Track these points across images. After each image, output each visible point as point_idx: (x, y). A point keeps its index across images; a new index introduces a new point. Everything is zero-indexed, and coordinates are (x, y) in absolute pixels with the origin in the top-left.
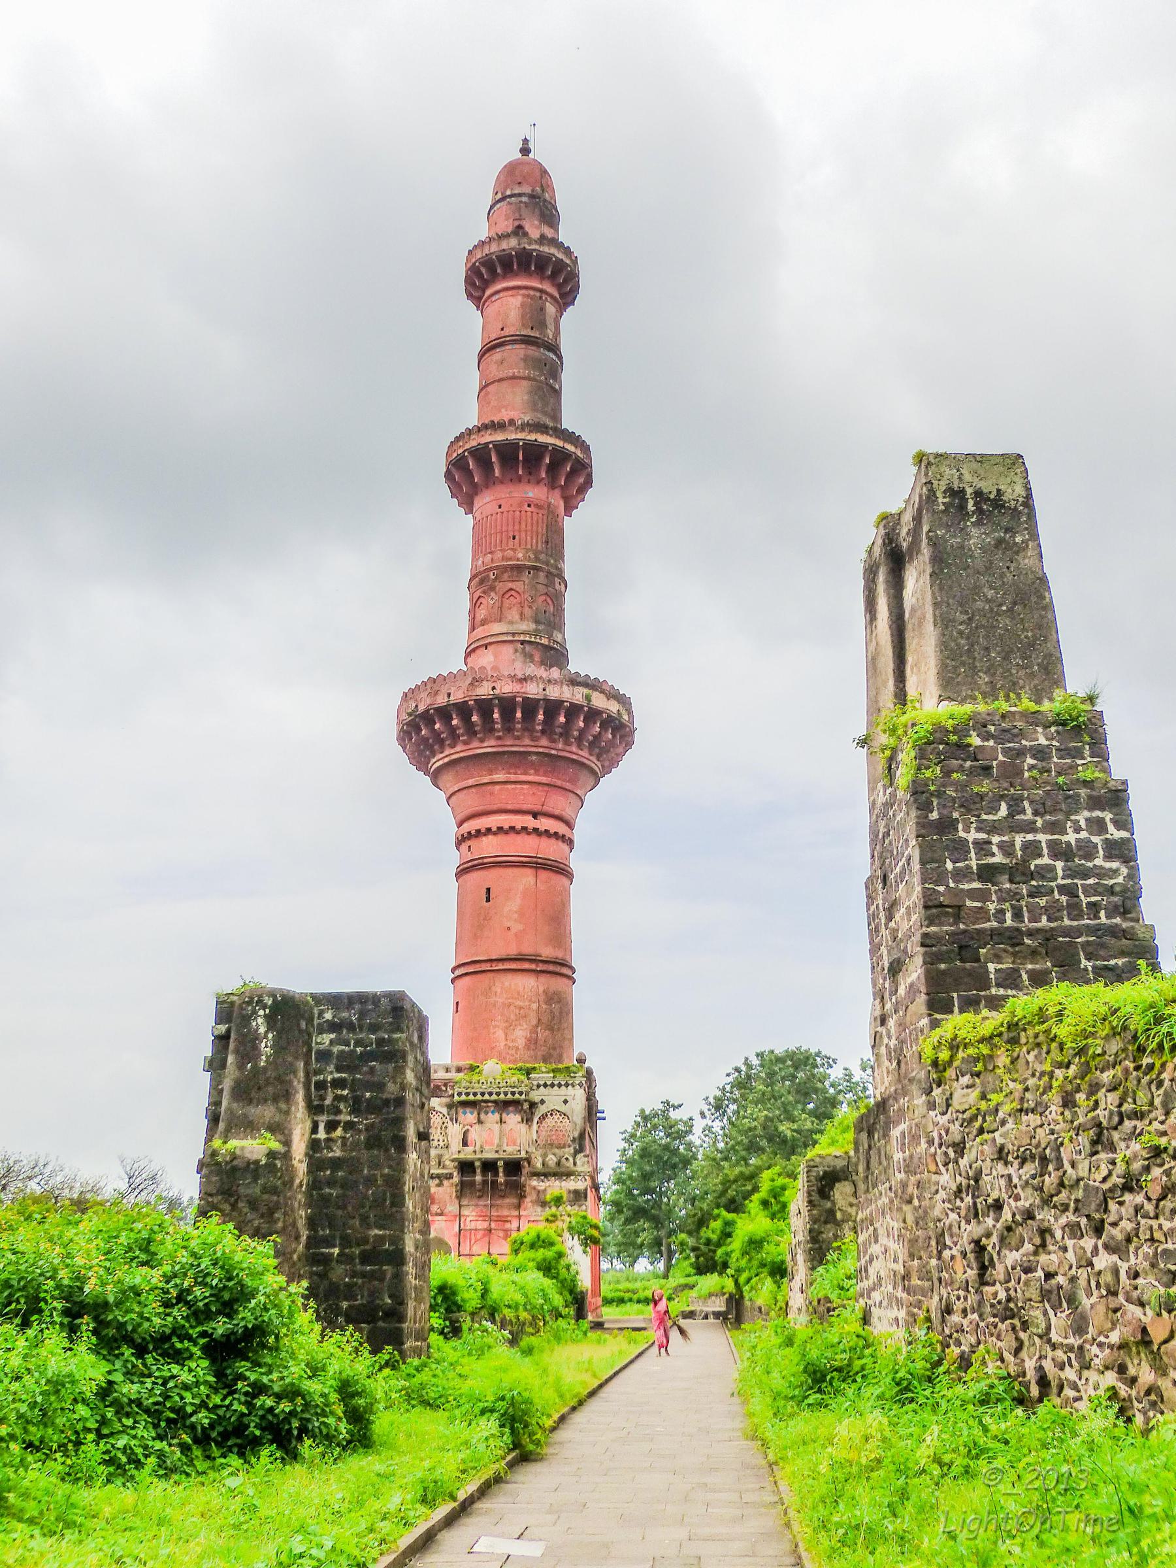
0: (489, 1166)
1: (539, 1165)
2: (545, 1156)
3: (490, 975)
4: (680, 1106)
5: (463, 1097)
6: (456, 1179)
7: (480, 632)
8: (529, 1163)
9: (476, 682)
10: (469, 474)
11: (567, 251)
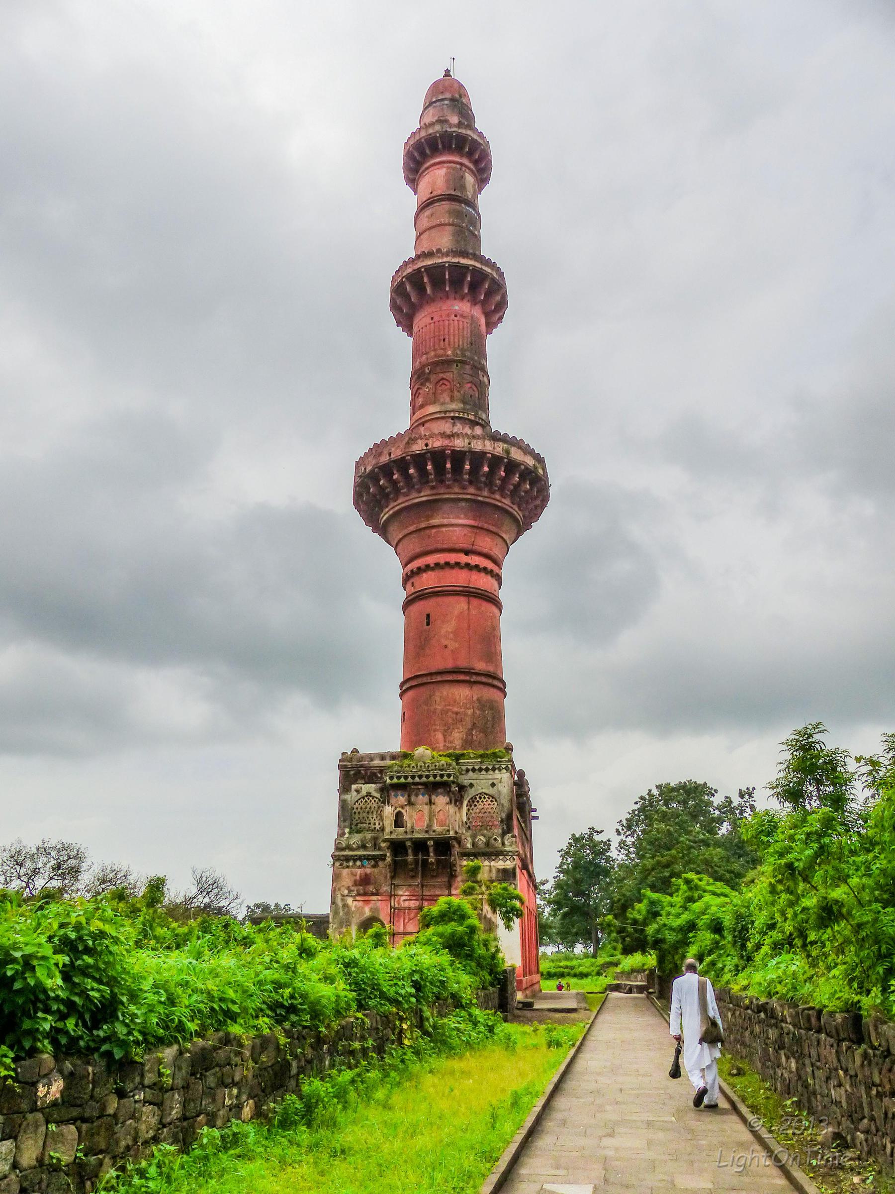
0: (420, 846)
1: (469, 845)
2: (474, 836)
3: (432, 686)
4: (602, 831)
5: (395, 780)
6: (389, 860)
7: (418, 415)
8: (459, 842)
9: (412, 441)
10: (407, 296)
11: (481, 134)
